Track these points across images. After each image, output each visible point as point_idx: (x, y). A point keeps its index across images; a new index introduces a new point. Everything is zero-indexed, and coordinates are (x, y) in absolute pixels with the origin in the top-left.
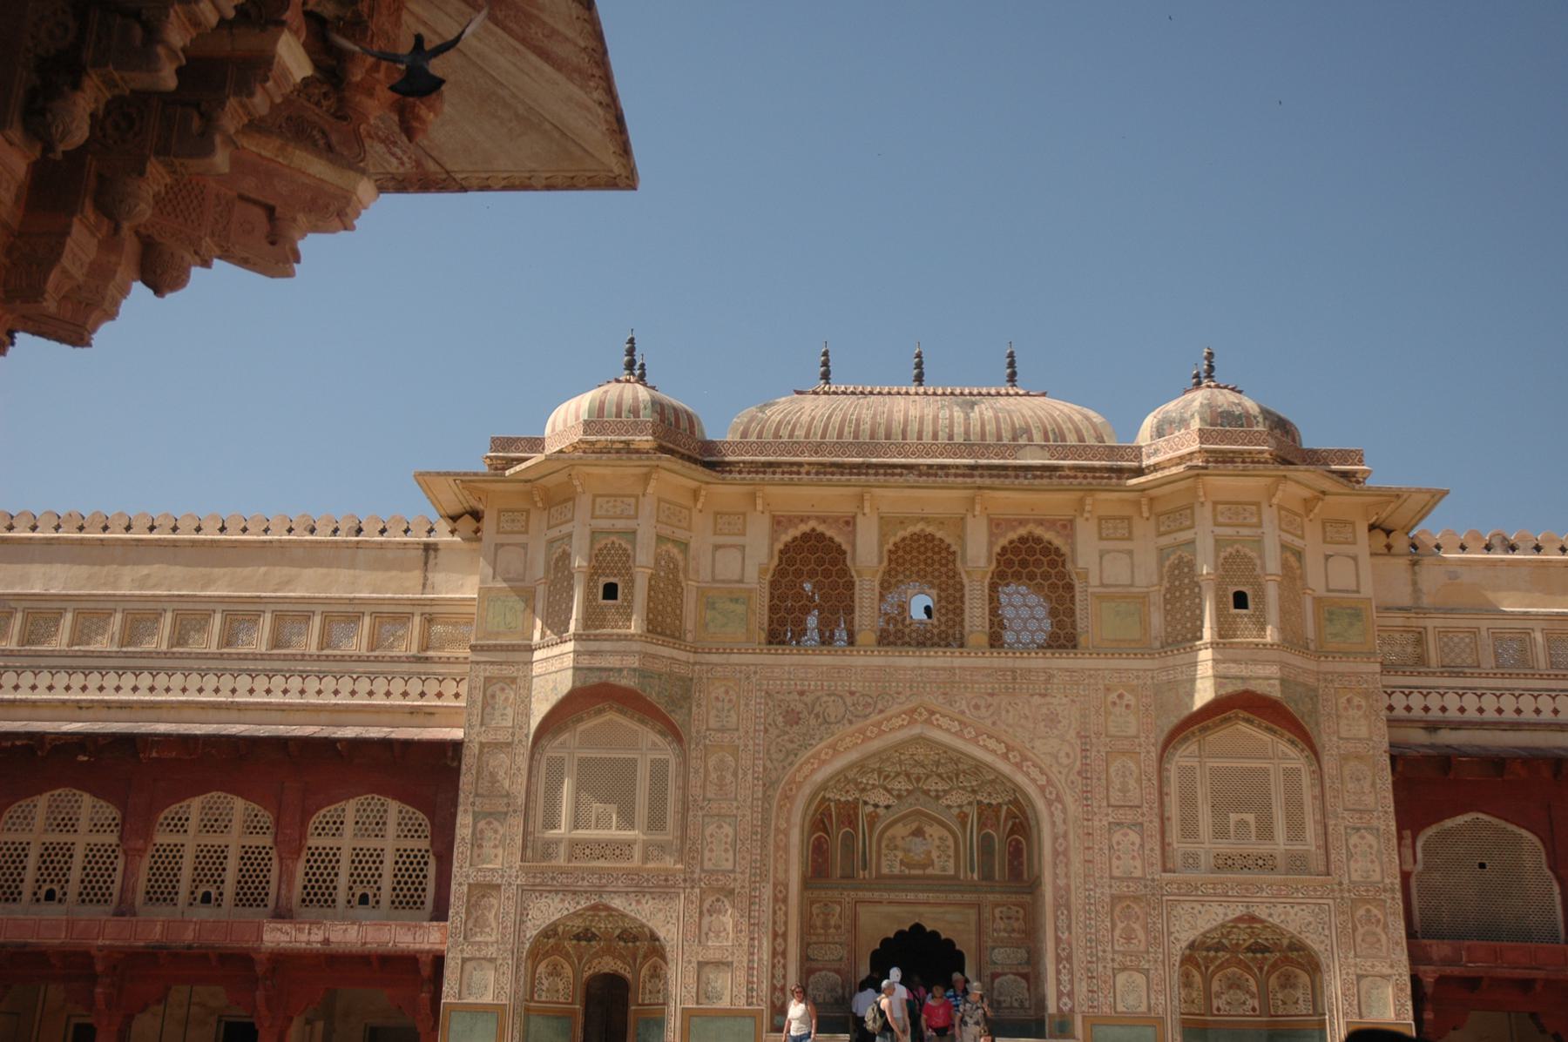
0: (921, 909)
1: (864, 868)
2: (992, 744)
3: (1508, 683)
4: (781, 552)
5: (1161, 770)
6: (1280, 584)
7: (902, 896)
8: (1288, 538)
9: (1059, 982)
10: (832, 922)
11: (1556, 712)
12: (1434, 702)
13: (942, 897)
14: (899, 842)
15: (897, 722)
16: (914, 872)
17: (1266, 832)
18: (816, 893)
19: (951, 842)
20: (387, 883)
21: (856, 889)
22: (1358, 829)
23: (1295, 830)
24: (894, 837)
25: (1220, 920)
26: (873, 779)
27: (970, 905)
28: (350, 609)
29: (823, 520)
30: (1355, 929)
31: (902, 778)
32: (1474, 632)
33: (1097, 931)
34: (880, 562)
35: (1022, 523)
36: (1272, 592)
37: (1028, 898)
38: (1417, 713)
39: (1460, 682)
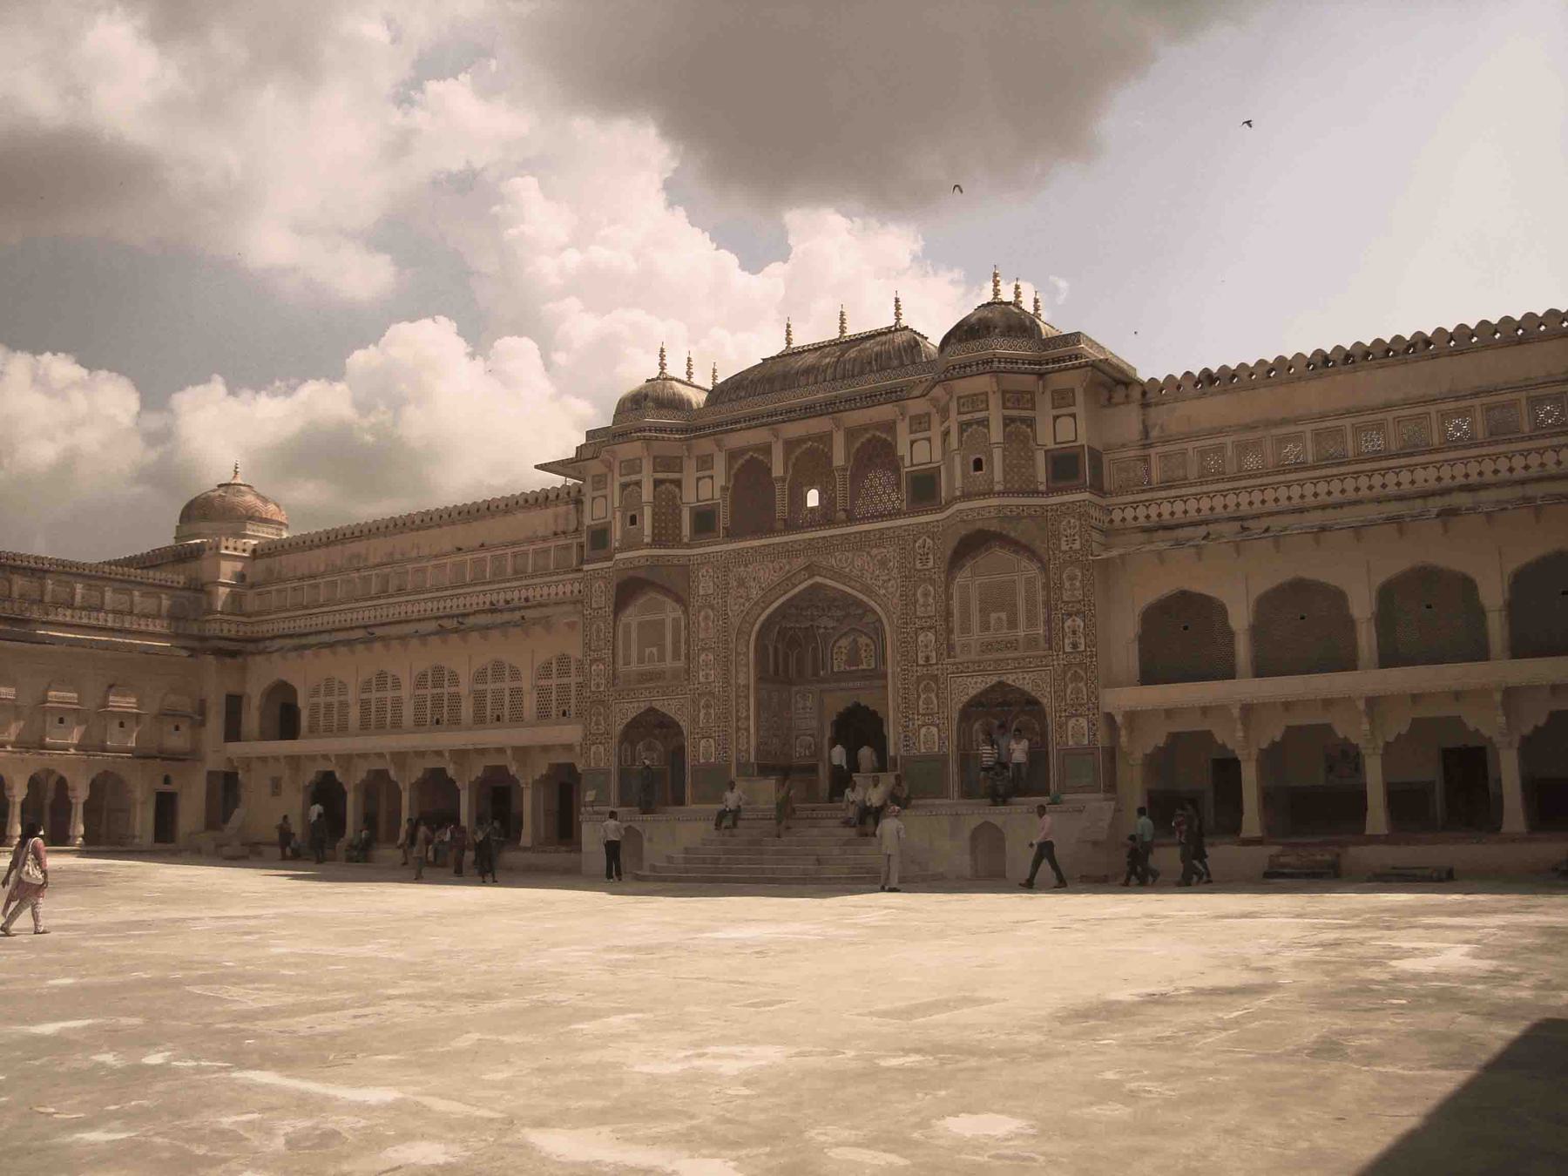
3: (1205, 488)
4: (736, 475)
5: (947, 587)
6: (1004, 450)
8: (1015, 413)
11: (1559, 463)
12: (1153, 511)
17: (1013, 624)
20: (573, 701)
22: (1070, 615)
23: (1031, 621)
25: (983, 687)
28: (546, 545)
29: (757, 449)
30: (1066, 686)
32: (1184, 453)
34: (786, 472)
35: (865, 428)
36: (997, 454)
38: (1142, 521)
39: (1173, 493)
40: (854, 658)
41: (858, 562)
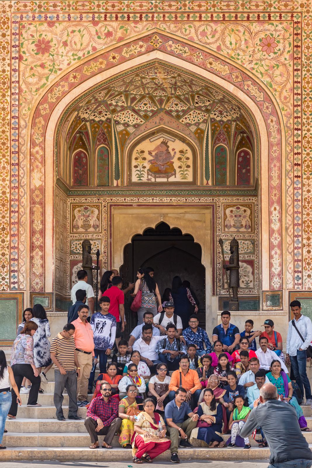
0: (165, 211)
1: (117, 179)
2: (217, 66)
7: (150, 200)
9: (271, 265)
10: (92, 223)
13: (182, 200)
14: (146, 155)
15: (135, 49)
16: (159, 180)
18: (78, 199)
19: (190, 154)
21: (110, 195)
24: (143, 152)
26: (121, 101)
27: (206, 207)
31: (147, 100)
33: (304, 222)
37: (253, 200)
40: (162, 165)
41: (230, 39)
